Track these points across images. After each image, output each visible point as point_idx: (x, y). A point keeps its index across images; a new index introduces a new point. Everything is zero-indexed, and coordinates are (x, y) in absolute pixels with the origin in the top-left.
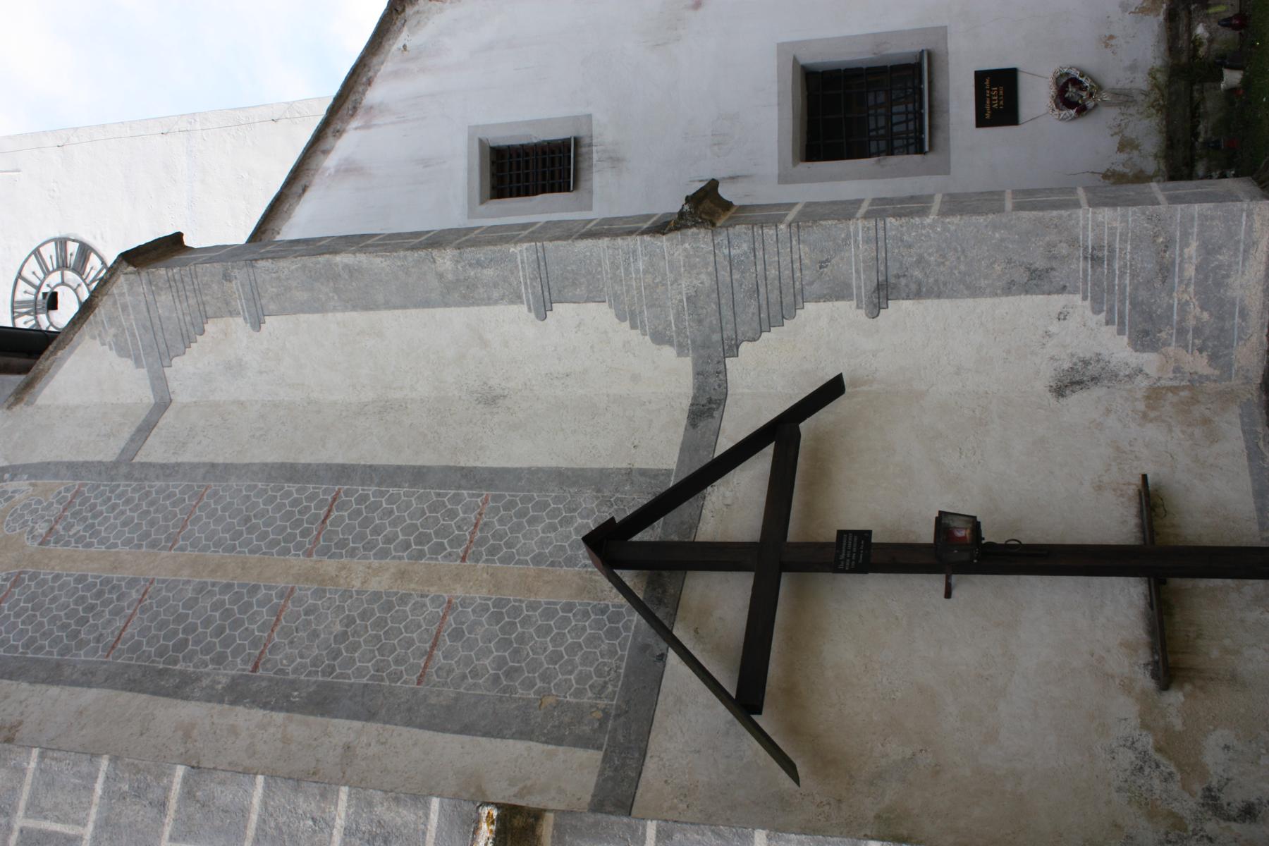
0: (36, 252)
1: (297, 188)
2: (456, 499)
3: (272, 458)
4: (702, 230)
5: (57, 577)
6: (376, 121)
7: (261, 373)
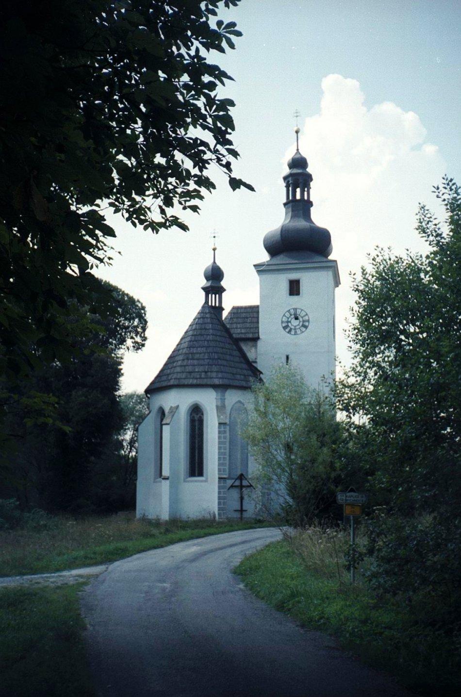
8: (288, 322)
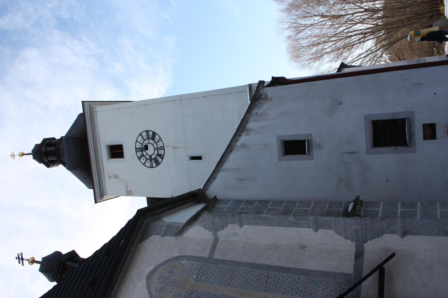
0: (141, 134)
1: (229, 150)
2: (299, 278)
3: (249, 261)
4: (358, 218)
5: (202, 292)
6: (250, 133)
7: (242, 236)
8: (151, 159)
